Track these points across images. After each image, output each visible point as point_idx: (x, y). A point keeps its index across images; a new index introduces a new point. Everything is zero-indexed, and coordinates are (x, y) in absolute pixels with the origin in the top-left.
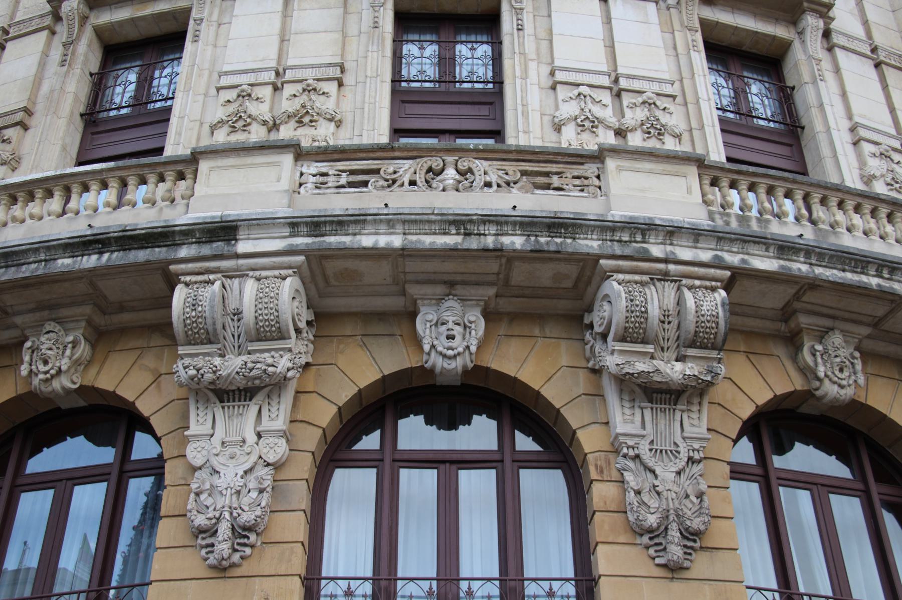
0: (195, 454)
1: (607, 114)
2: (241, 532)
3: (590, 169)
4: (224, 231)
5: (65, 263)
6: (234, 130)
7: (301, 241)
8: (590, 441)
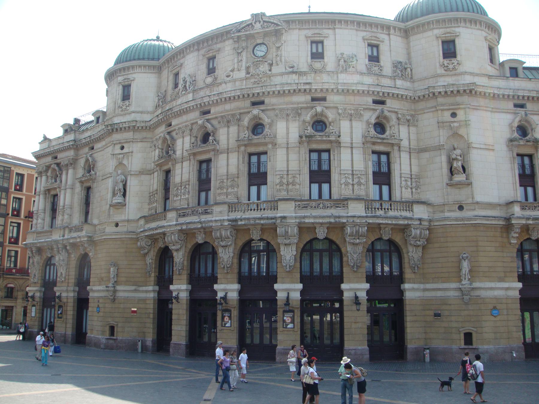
0: (282, 253)
1: (350, 181)
2: (290, 266)
3: (346, 203)
4: (284, 218)
6: (280, 186)
7: (297, 221)
8: (343, 250)
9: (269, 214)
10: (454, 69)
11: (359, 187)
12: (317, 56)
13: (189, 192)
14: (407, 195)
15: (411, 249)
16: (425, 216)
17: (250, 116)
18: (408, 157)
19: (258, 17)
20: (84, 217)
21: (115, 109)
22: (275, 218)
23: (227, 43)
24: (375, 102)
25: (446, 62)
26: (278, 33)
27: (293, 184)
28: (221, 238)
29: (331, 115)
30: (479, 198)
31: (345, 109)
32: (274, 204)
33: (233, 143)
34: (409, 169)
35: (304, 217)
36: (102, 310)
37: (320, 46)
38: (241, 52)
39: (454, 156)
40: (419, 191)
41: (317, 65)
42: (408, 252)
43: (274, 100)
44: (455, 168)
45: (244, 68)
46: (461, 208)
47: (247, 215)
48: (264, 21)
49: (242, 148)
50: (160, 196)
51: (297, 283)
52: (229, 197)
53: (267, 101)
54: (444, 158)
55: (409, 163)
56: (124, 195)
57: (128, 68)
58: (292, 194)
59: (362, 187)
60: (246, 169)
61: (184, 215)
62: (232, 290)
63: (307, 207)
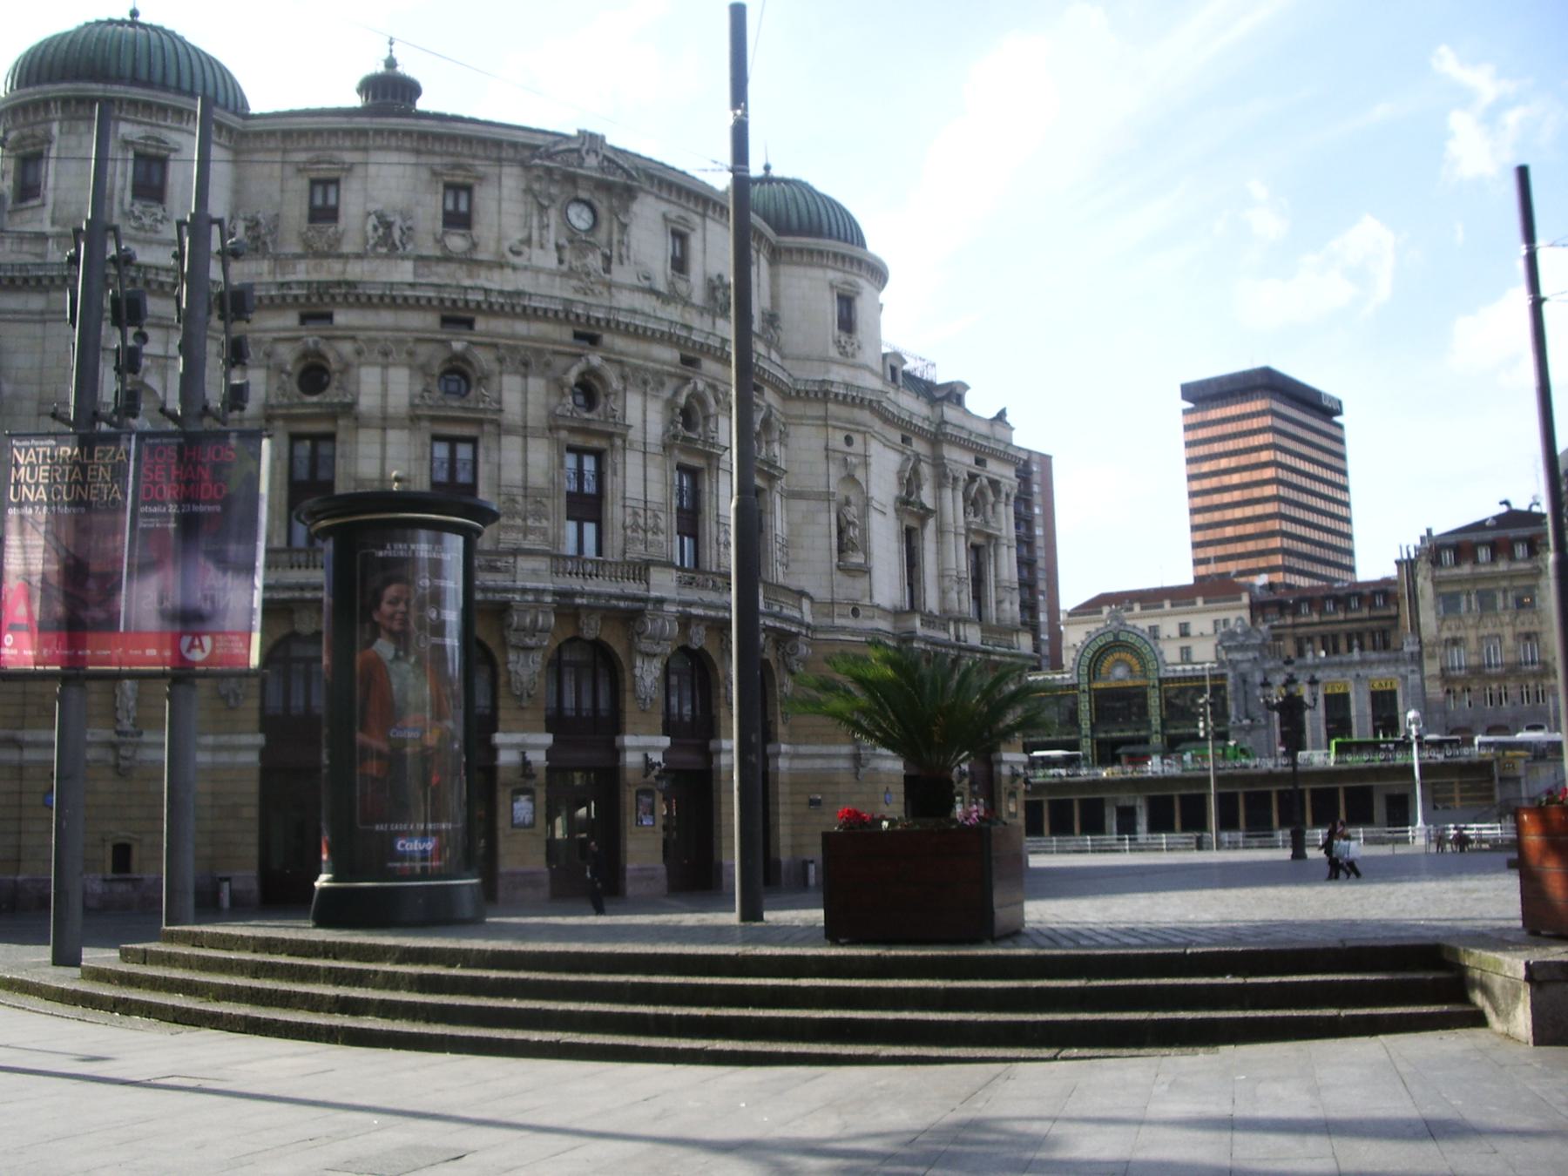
0: (638, 672)
4: (660, 601)
5: (614, 602)
9: (633, 588)
10: (853, 355)
12: (680, 264)
19: (591, 141)
22: (646, 600)
23: (507, 170)
26: (628, 193)
28: (534, 630)
30: (878, 599)
32: (640, 570)
33: (537, 415)
35: (691, 604)
39: (850, 518)
42: (782, 685)
43: (619, 343)
44: (850, 539)
45: (552, 246)
46: (855, 613)
47: (592, 585)
49: (563, 434)
53: (607, 338)
57: (163, 109)
62: (536, 747)
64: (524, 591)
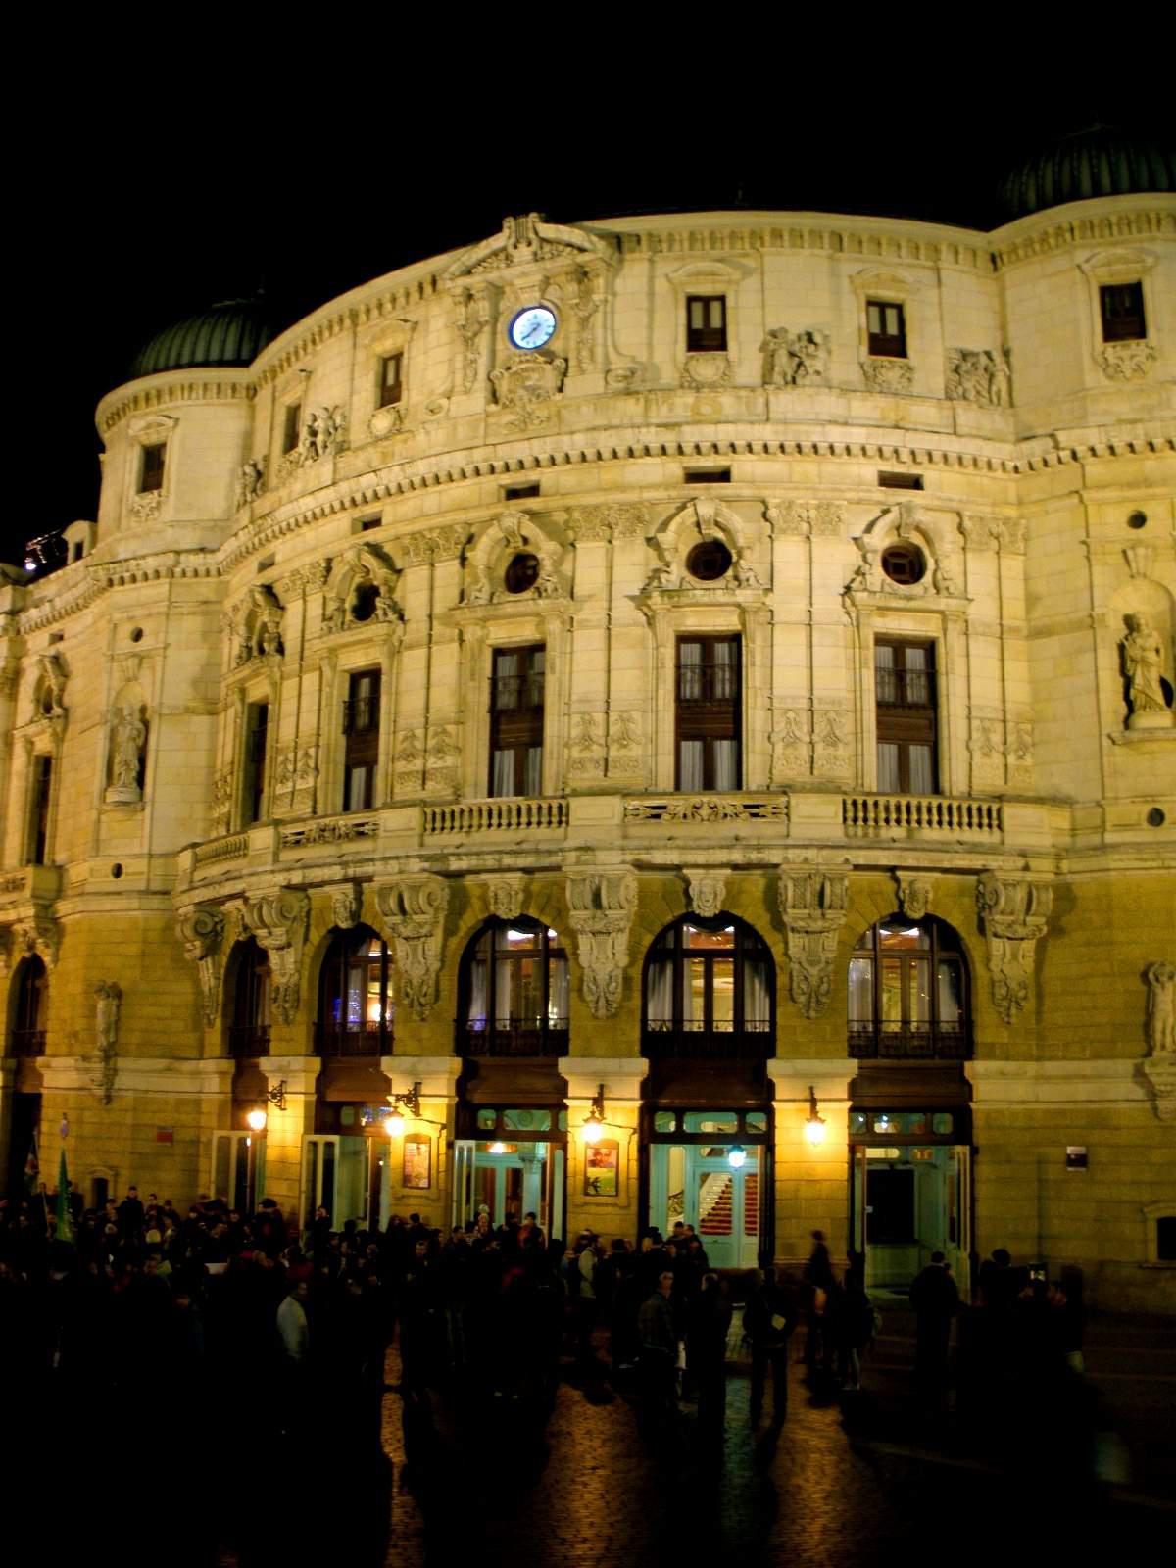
0: (584, 960)
8: (777, 951)
11: (831, 750)
13: (317, 769)
14: (989, 776)
15: (996, 944)
16: (1045, 841)
17: (494, 532)
18: (996, 653)
20: (34, 847)
21: (119, 519)
23: (435, 309)
24: (888, 481)
25: (1114, 351)
27: (624, 739)
29: (742, 528)
31: (790, 505)
34: (997, 693)
36: (74, 1130)
37: (716, 307)
38: (476, 335)
40: (1029, 761)
41: (707, 366)
48: (544, 240)
50: (236, 784)
51: (630, 1056)
52: (430, 785)
54: (1109, 660)
55: (997, 674)
56: (140, 780)
58: (617, 777)
59: (842, 751)
60: (485, 698)
61: (298, 842)
63: (658, 817)
64: (385, 859)
